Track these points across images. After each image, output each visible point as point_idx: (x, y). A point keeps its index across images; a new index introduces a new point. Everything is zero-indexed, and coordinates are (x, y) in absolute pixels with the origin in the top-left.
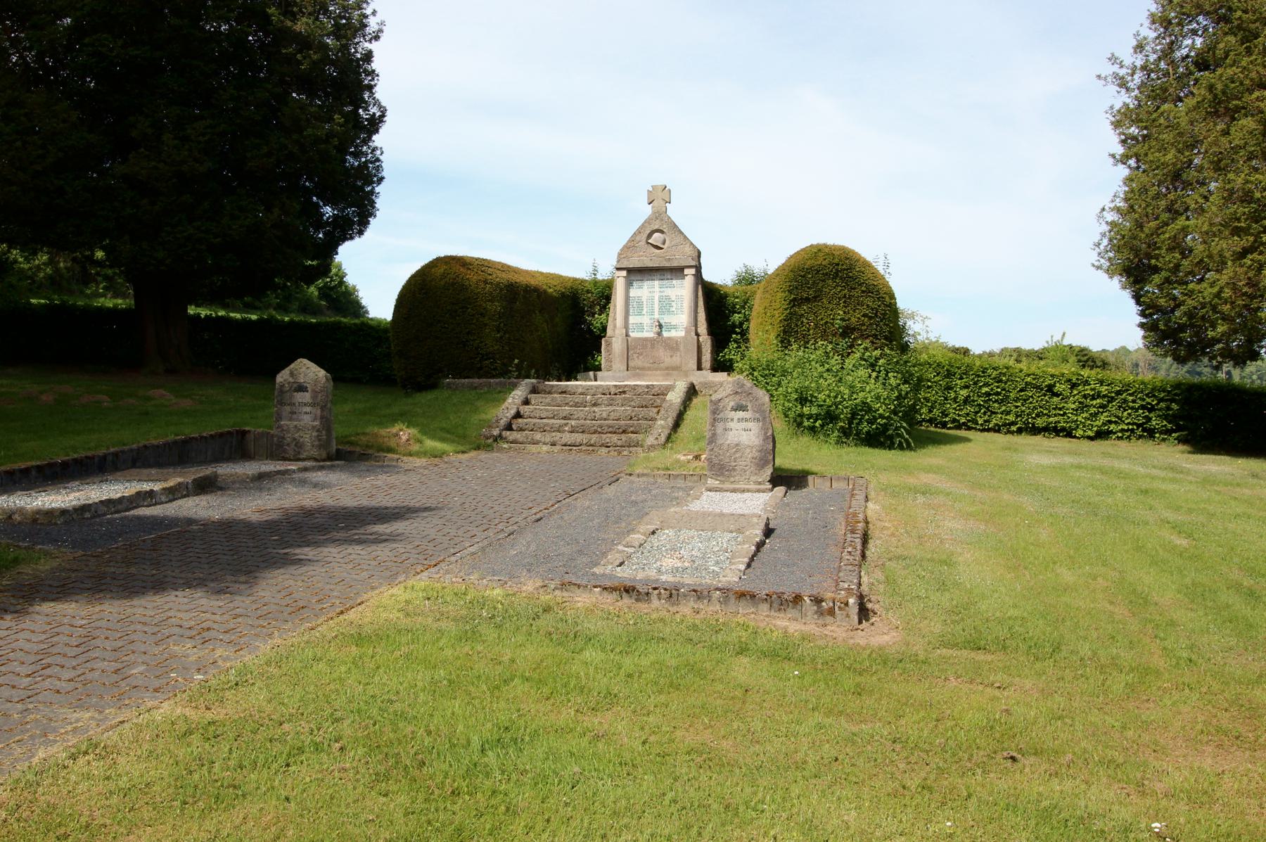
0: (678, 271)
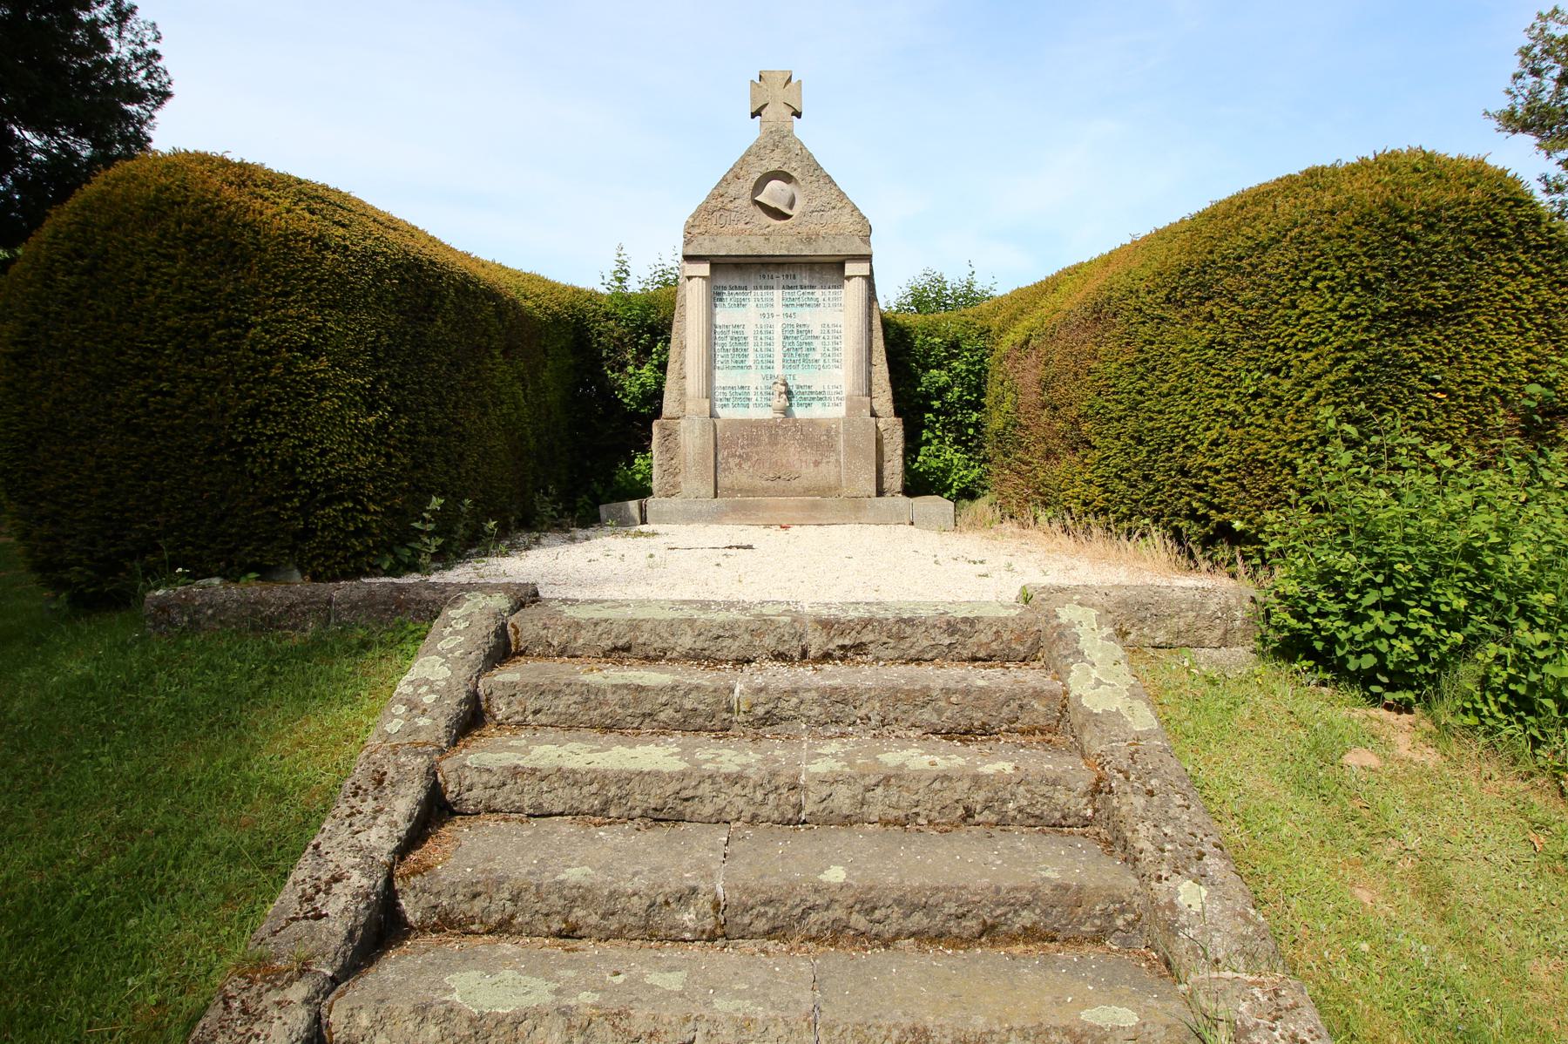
0: (830, 269)
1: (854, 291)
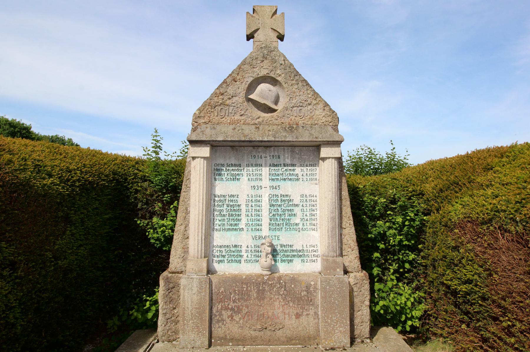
0: (309, 151)
1: (327, 171)
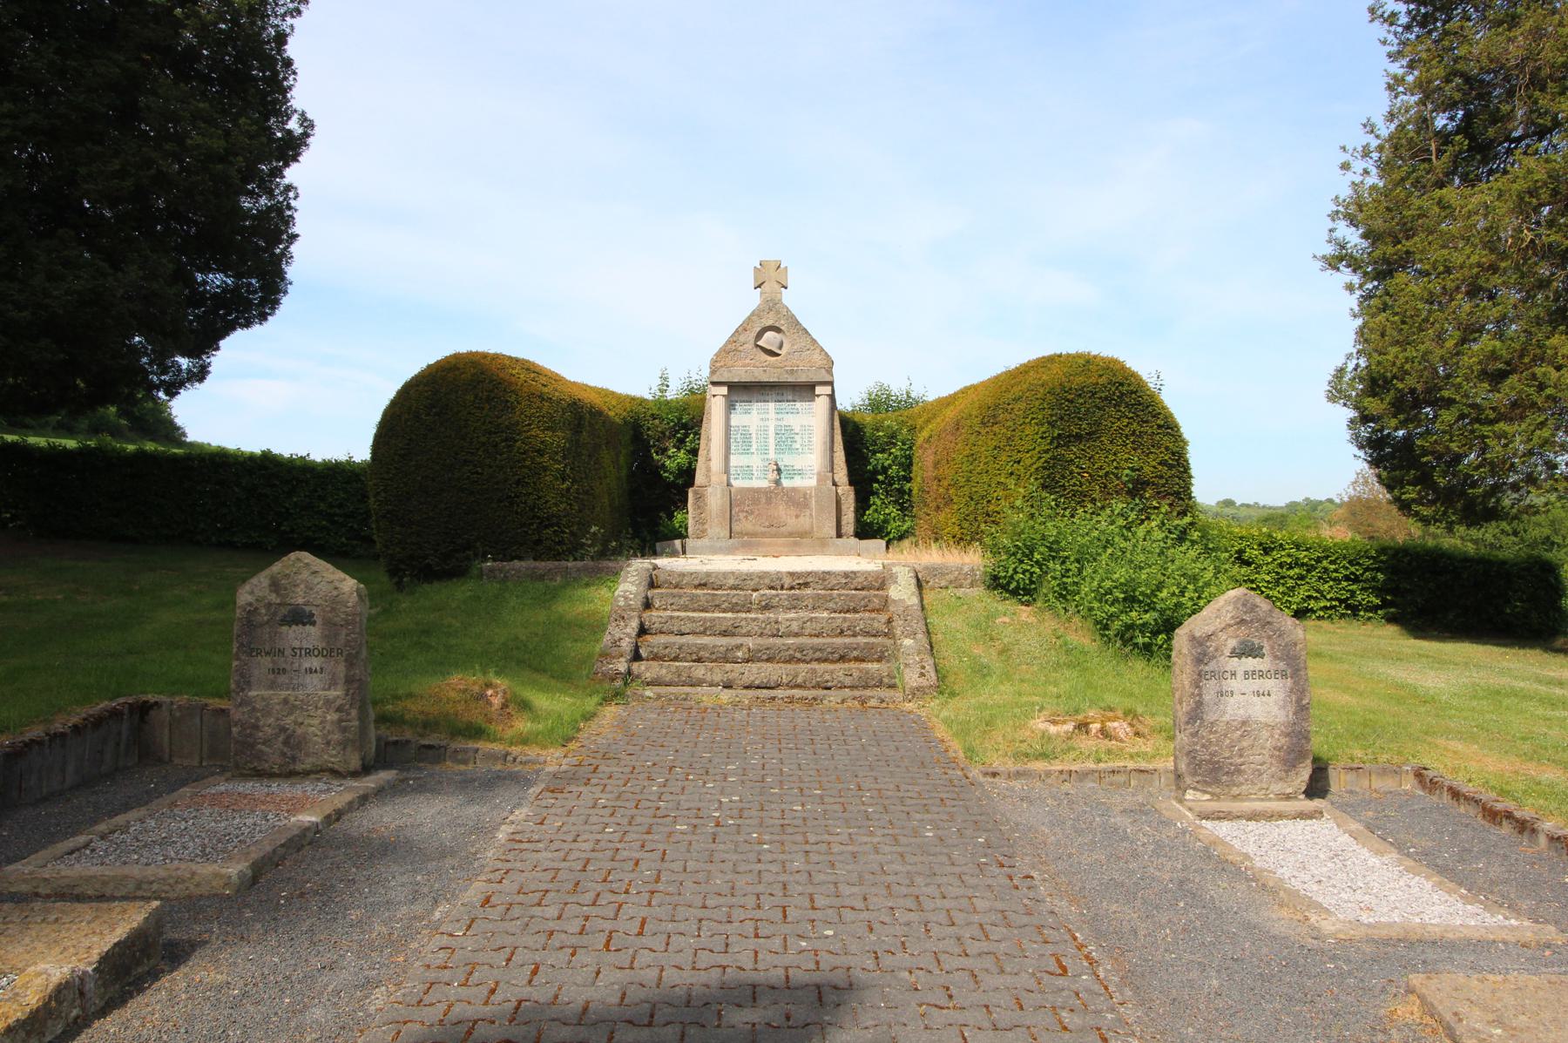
0: (805, 390)
1: (821, 404)
